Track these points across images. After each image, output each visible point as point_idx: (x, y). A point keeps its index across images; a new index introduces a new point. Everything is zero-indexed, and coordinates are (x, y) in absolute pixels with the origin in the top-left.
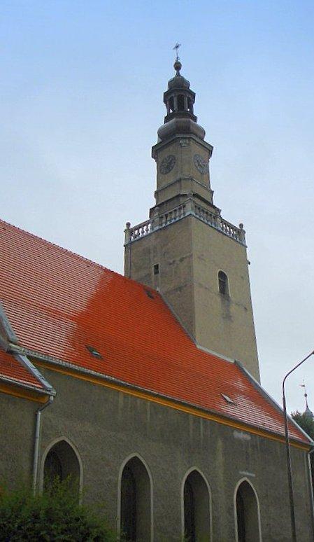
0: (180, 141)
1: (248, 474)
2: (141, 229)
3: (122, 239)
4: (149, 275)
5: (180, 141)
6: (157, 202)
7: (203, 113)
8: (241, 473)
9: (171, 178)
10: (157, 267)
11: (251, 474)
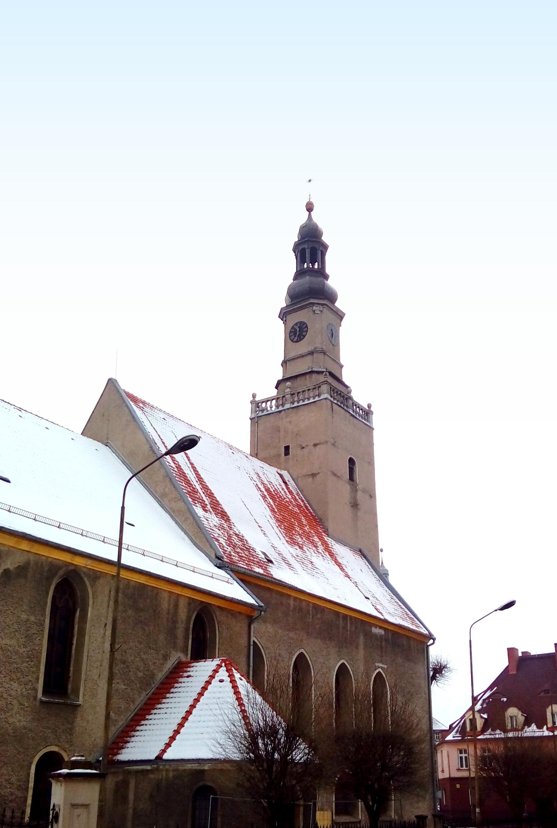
0: (310, 297)
1: (381, 665)
2: (269, 403)
3: (247, 412)
4: (279, 455)
5: (310, 297)
6: (284, 372)
7: (338, 272)
8: (377, 664)
9: (303, 347)
10: (287, 448)
11: (383, 666)
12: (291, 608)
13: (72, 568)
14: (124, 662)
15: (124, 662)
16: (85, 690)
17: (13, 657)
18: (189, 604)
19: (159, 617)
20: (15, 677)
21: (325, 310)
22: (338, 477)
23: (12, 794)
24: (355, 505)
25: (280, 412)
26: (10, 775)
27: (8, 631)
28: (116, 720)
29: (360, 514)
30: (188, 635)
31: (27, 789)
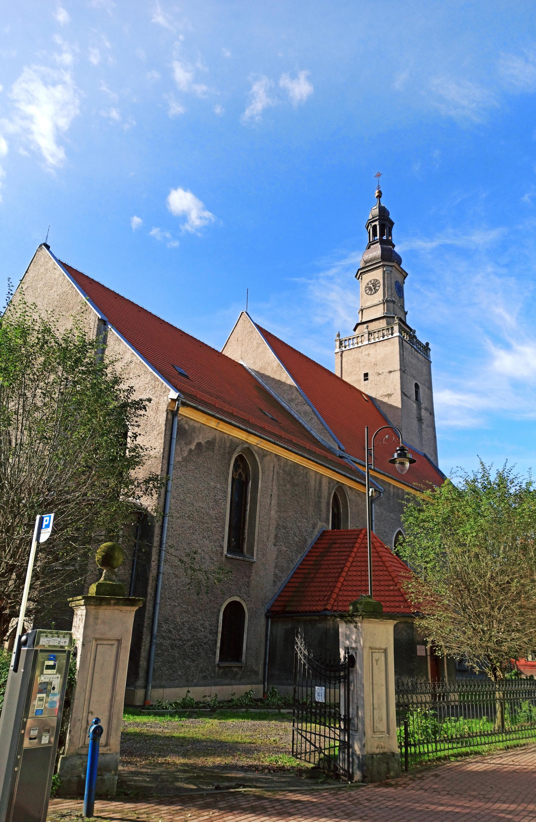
10: (366, 375)
12: (392, 494)
13: (246, 446)
14: (285, 528)
15: (285, 528)
16: (258, 550)
17: (205, 518)
18: (329, 483)
19: (309, 493)
20: (207, 536)
21: (394, 270)
22: (408, 397)
23: (206, 637)
24: (420, 419)
25: (360, 347)
26: (204, 620)
27: (201, 496)
28: (280, 577)
29: (424, 426)
30: (329, 509)
31: (217, 633)
